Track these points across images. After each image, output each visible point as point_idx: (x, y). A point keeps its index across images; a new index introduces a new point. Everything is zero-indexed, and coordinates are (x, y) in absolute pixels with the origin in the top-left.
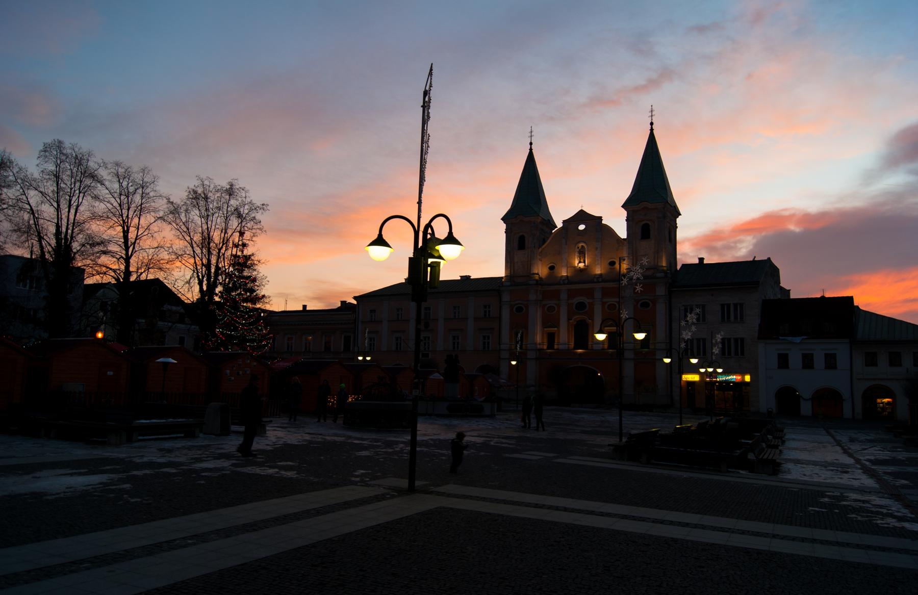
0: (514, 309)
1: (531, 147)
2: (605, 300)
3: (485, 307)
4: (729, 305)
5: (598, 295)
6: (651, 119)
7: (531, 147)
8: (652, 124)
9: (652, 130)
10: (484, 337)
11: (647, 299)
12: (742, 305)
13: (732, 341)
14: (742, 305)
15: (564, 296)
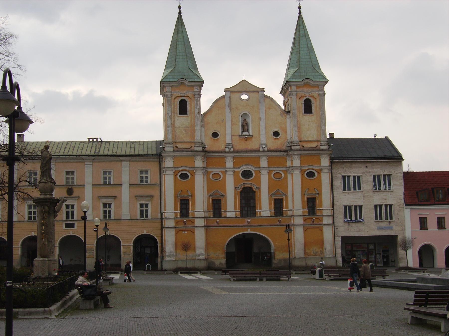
0: (178, 176)
1: (180, 11)
2: (270, 169)
3: (142, 172)
4: (379, 176)
5: (264, 163)
6: (298, 3)
7: (180, 11)
8: (300, 8)
9: (300, 13)
10: (142, 205)
11: (307, 170)
12: (389, 176)
13: (383, 208)
14: (389, 176)
15: (229, 163)
